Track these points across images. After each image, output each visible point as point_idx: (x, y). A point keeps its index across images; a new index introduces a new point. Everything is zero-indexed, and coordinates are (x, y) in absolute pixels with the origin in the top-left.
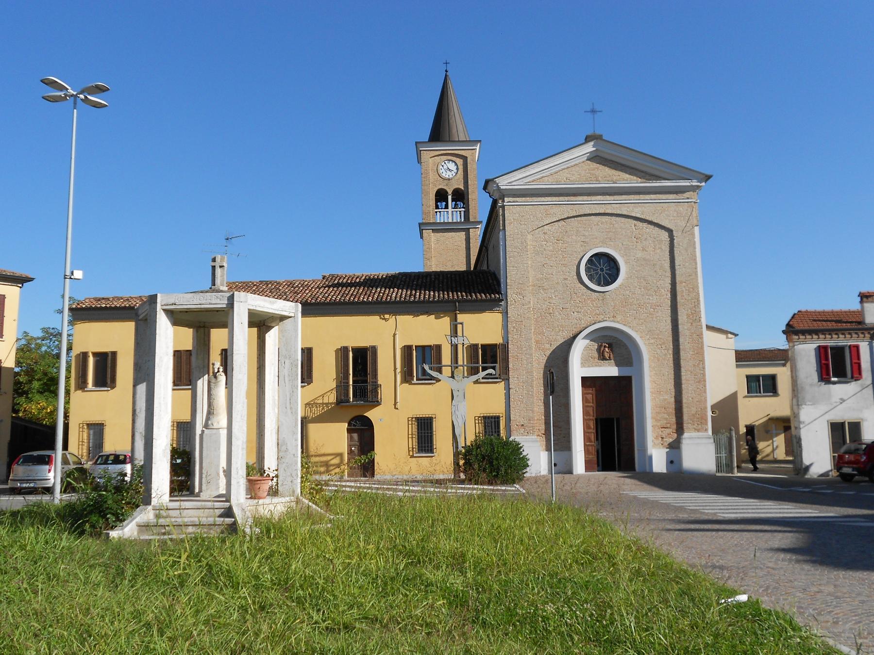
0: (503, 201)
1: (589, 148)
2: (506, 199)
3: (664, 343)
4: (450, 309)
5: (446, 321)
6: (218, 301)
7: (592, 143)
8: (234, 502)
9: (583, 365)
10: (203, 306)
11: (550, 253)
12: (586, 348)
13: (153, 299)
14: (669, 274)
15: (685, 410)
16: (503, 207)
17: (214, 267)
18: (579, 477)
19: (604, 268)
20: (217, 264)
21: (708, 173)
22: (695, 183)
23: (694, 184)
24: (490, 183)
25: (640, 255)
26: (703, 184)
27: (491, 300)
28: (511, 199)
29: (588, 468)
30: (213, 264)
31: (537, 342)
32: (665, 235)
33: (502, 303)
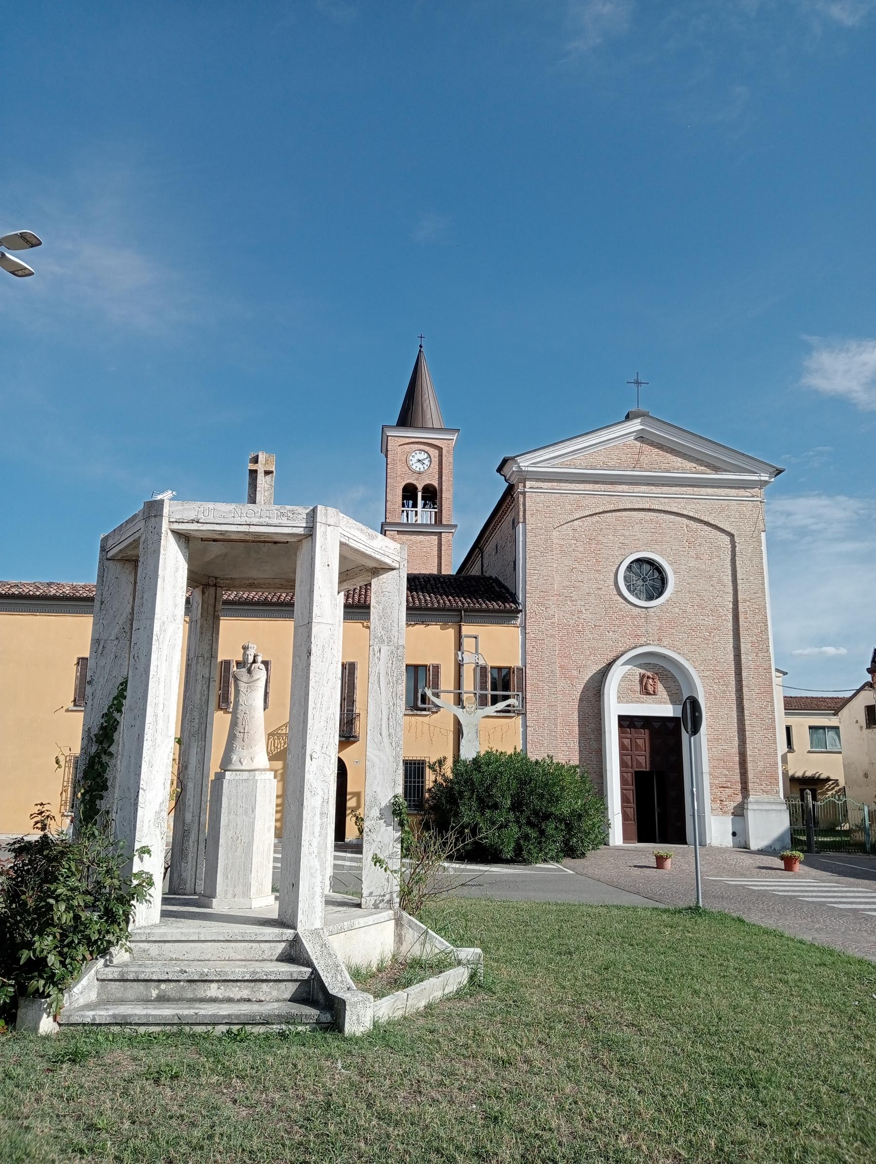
0: (524, 487)
1: (636, 425)
2: (528, 484)
3: (722, 677)
4: (457, 617)
5: (451, 632)
6: (284, 521)
7: (639, 420)
8: (302, 929)
9: (620, 700)
10: (253, 529)
11: (580, 556)
12: (624, 678)
13: (154, 509)
14: (730, 589)
15: (750, 766)
16: (524, 493)
17: (253, 473)
18: (618, 849)
19: (650, 578)
20: (260, 468)
21: (780, 467)
22: (765, 477)
23: (763, 478)
24: (509, 462)
25: (693, 563)
26: (773, 480)
27: (505, 611)
28: (534, 484)
29: (626, 838)
30: (252, 467)
31: (561, 667)
32: (727, 539)
33: (520, 615)
